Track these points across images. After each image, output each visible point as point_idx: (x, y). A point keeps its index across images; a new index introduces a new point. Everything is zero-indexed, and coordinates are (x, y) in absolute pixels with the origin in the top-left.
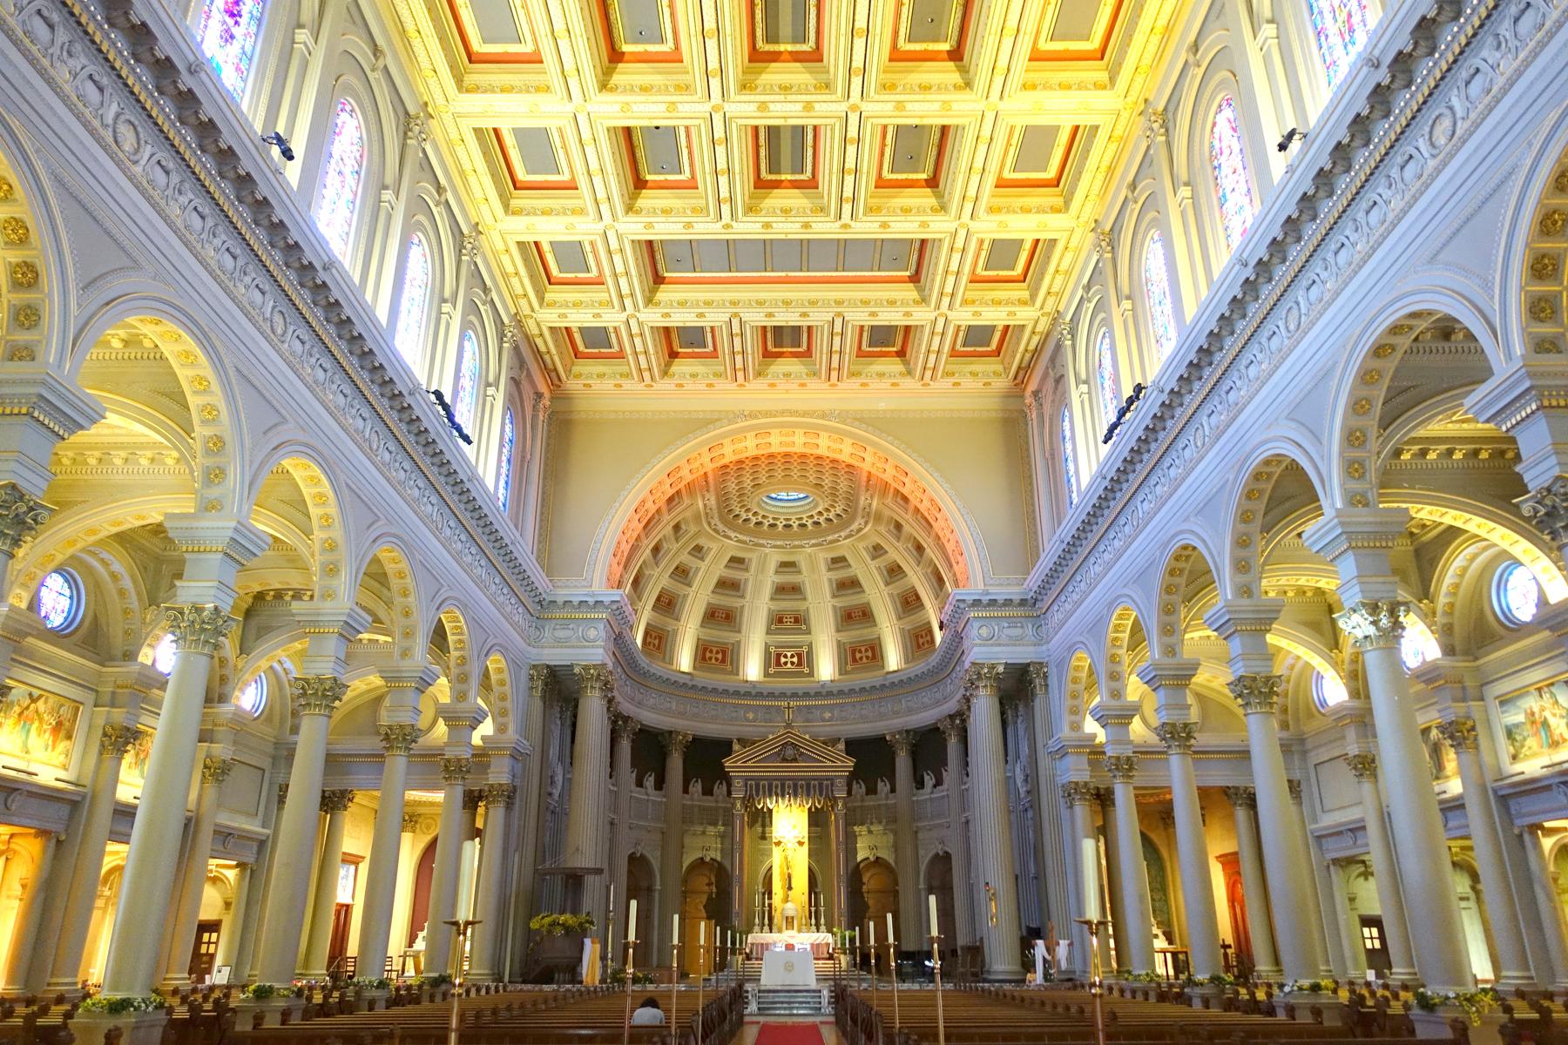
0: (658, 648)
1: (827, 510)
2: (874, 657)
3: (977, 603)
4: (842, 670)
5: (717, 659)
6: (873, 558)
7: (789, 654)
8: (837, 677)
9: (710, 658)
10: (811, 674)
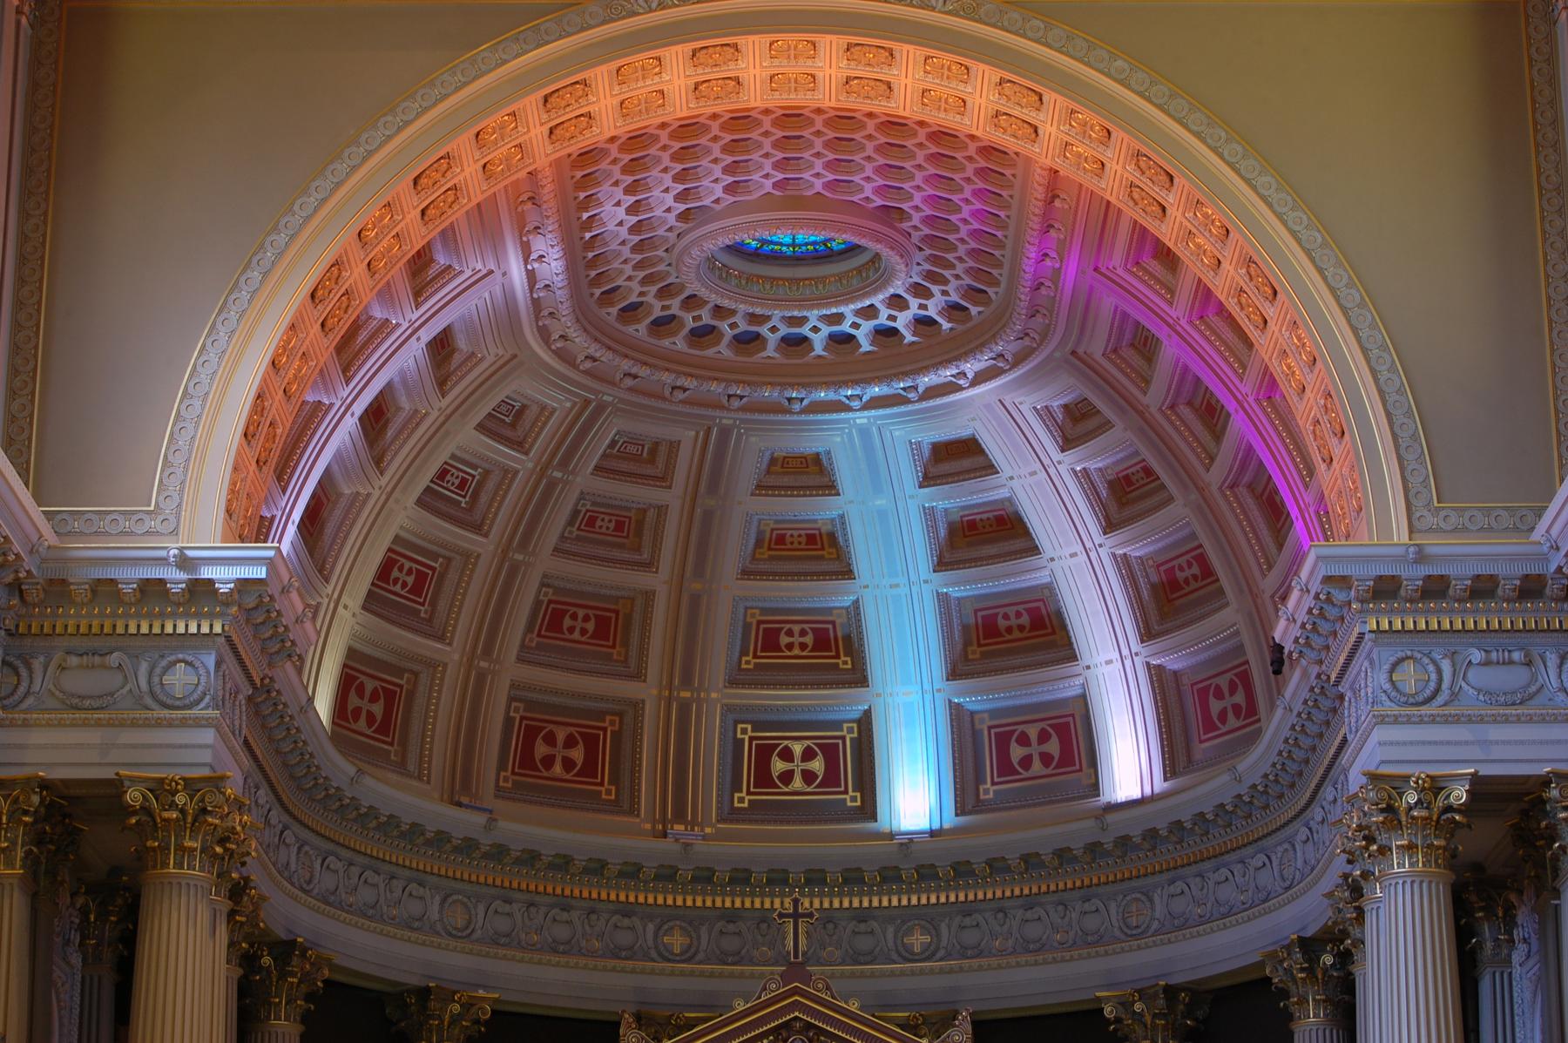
0: (385, 727)
1: (920, 291)
2: (1067, 758)
3: (1385, 590)
4: (966, 793)
5: (568, 764)
6: (1067, 444)
7: (797, 749)
8: (950, 820)
9: (548, 761)
10: (868, 809)
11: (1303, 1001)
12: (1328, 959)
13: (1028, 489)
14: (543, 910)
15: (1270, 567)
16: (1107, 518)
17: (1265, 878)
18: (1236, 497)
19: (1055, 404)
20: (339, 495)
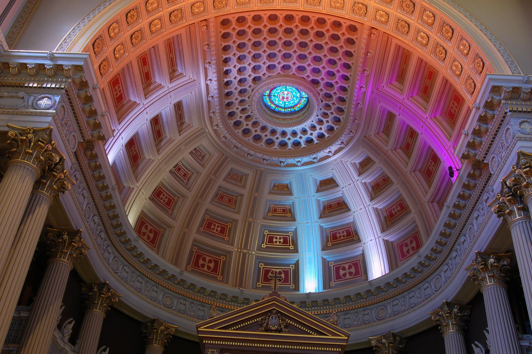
1: (320, 122)
2: (357, 273)
4: (326, 281)
5: (209, 268)
6: (360, 174)
8: (321, 290)
9: (203, 266)
10: (297, 288)
11: (447, 325)
12: (455, 310)
13: (348, 190)
14: (196, 305)
15: (427, 194)
16: (371, 197)
17: (428, 291)
18: (415, 174)
19: (357, 162)
20: (145, 158)
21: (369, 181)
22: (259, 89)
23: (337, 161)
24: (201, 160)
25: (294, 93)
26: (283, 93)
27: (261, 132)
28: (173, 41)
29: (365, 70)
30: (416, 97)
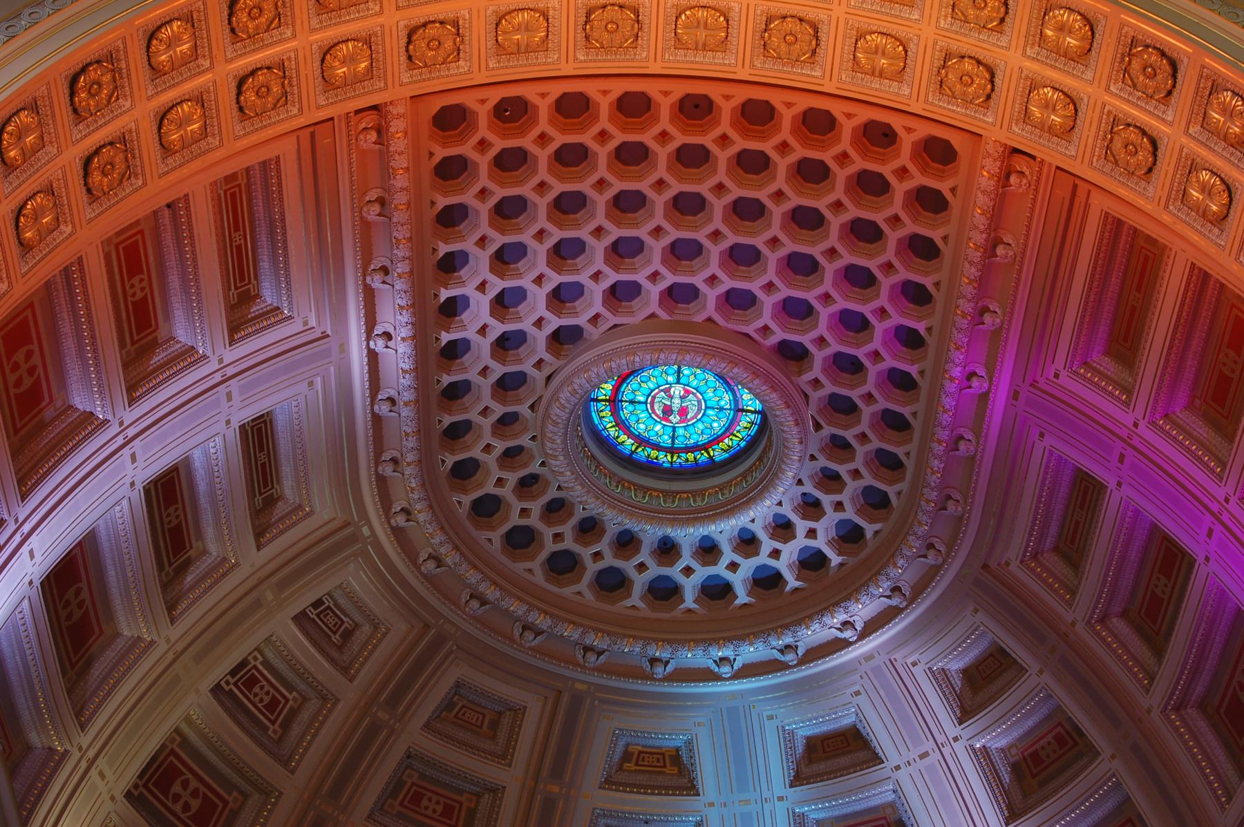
1: (811, 508)
6: (965, 714)
13: (918, 779)
16: (1010, 807)
18: (1183, 720)
19: (955, 665)
20: (118, 635)
21: (1002, 743)
22: (575, 373)
23: (872, 663)
24: (340, 648)
25: (710, 394)
26: (667, 391)
27: (576, 540)
28: (248, 186)
29: (986, 309)
30: (1183, 416)
